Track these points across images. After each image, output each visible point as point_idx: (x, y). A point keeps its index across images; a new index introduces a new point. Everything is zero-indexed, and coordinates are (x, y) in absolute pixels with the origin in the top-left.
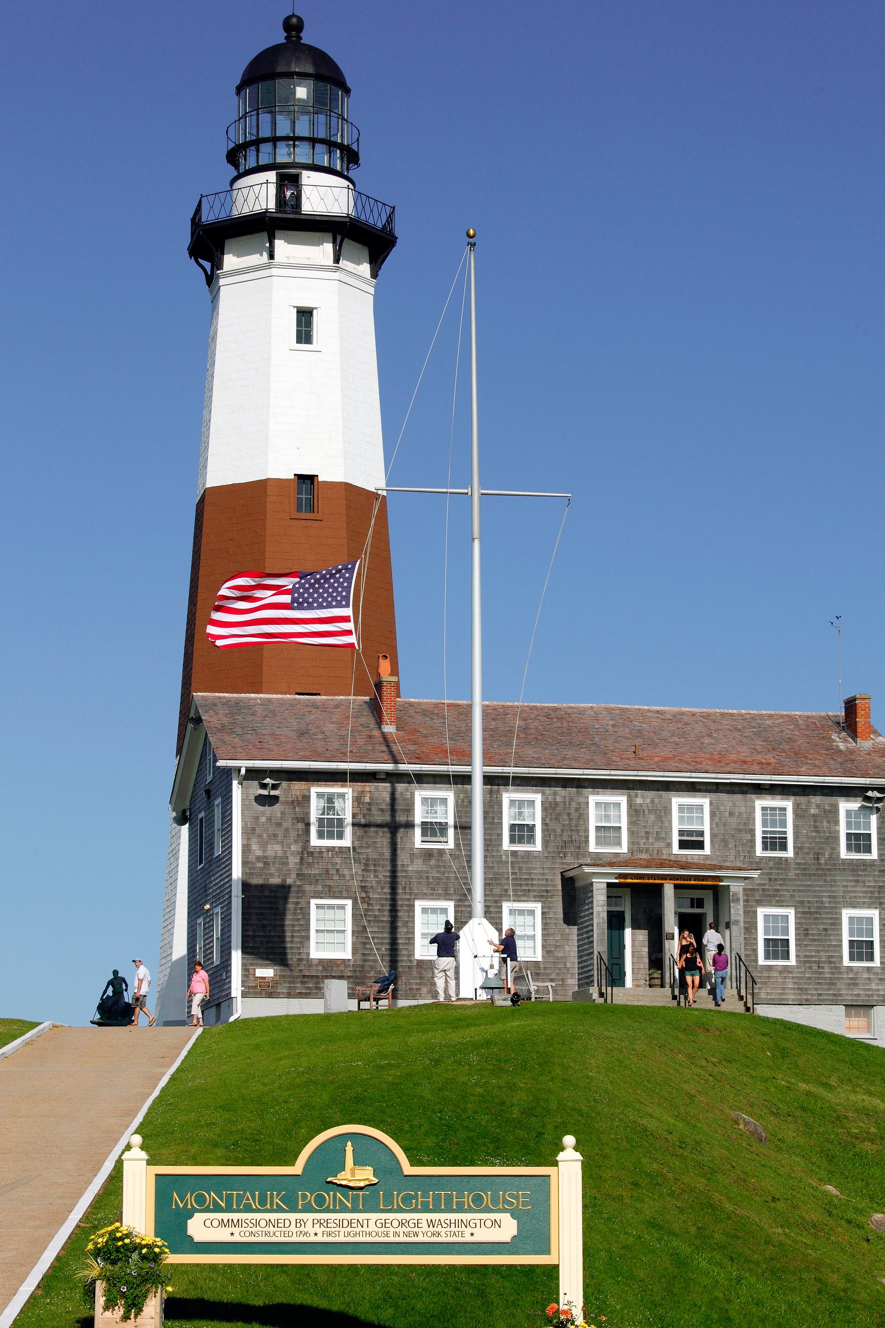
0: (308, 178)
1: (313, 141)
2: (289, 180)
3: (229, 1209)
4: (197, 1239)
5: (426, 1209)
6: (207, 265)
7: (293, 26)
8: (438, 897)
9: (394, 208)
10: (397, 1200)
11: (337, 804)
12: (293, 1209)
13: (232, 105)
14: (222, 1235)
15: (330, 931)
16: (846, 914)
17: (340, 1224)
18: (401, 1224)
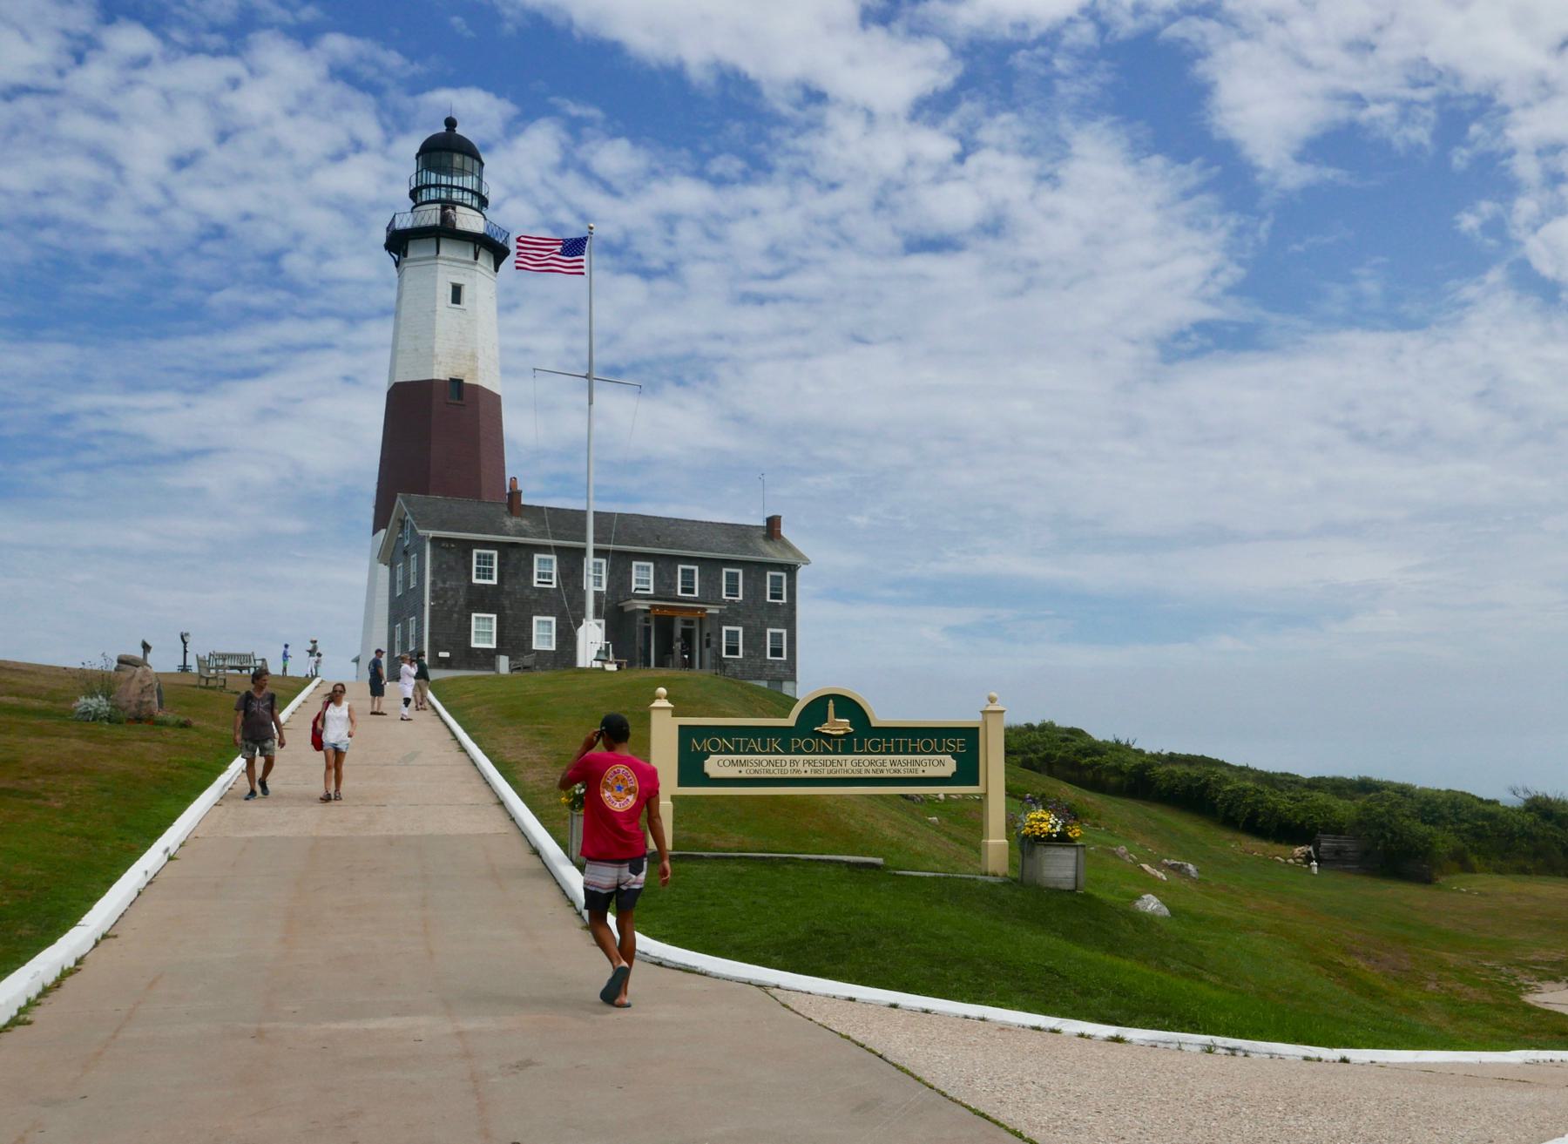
0: (459, 208)
1: (463, 189)
3: (737, 752)
4: (713, 775)
5: (888, 752)
10: (868, 743)
12: (788, 752)
13: (412, 166)
14: (732, 772)
15: (483, 632)
16: (769, 631)
17: (824, 764)
18: (871, 763)
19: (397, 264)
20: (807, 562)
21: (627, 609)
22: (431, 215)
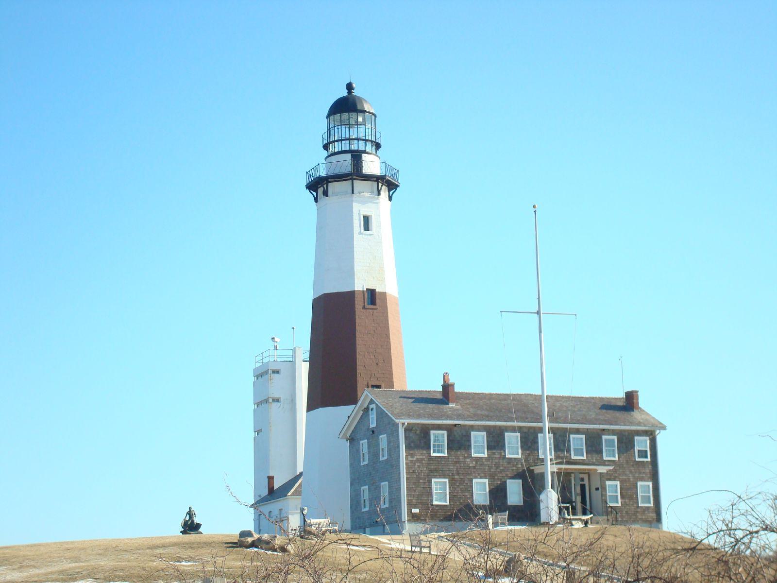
2: (357, 156)
6: (315, 194)
7: (350, 87)
8: (481, 478)
9: (398, 171)
11: (440, 438)
16: (639, 484)
19: (316, 200)
20: (663, 428)
21: (536, 472)
22: (345, 163)
